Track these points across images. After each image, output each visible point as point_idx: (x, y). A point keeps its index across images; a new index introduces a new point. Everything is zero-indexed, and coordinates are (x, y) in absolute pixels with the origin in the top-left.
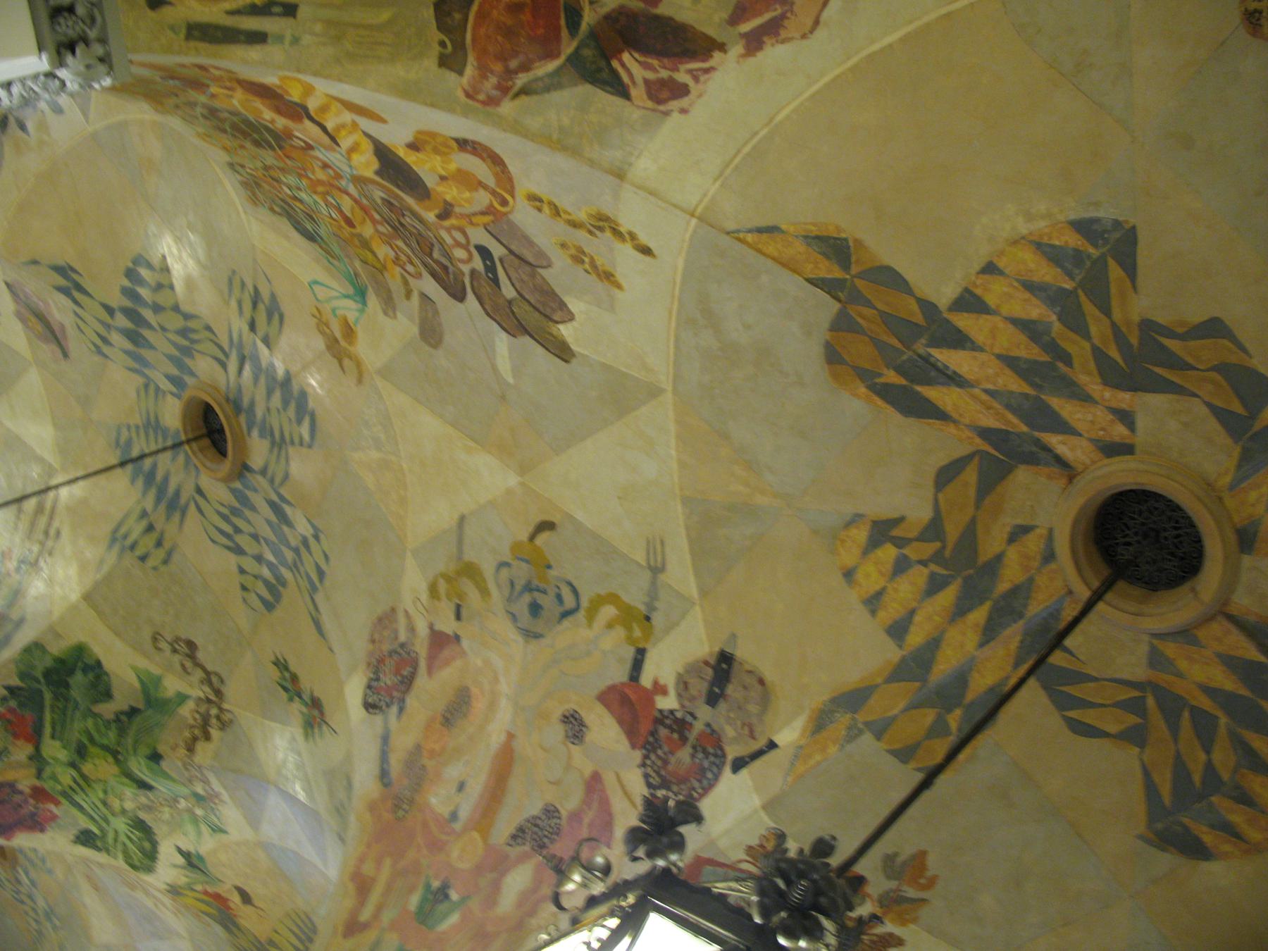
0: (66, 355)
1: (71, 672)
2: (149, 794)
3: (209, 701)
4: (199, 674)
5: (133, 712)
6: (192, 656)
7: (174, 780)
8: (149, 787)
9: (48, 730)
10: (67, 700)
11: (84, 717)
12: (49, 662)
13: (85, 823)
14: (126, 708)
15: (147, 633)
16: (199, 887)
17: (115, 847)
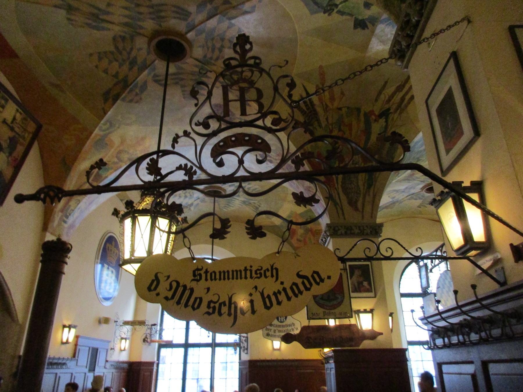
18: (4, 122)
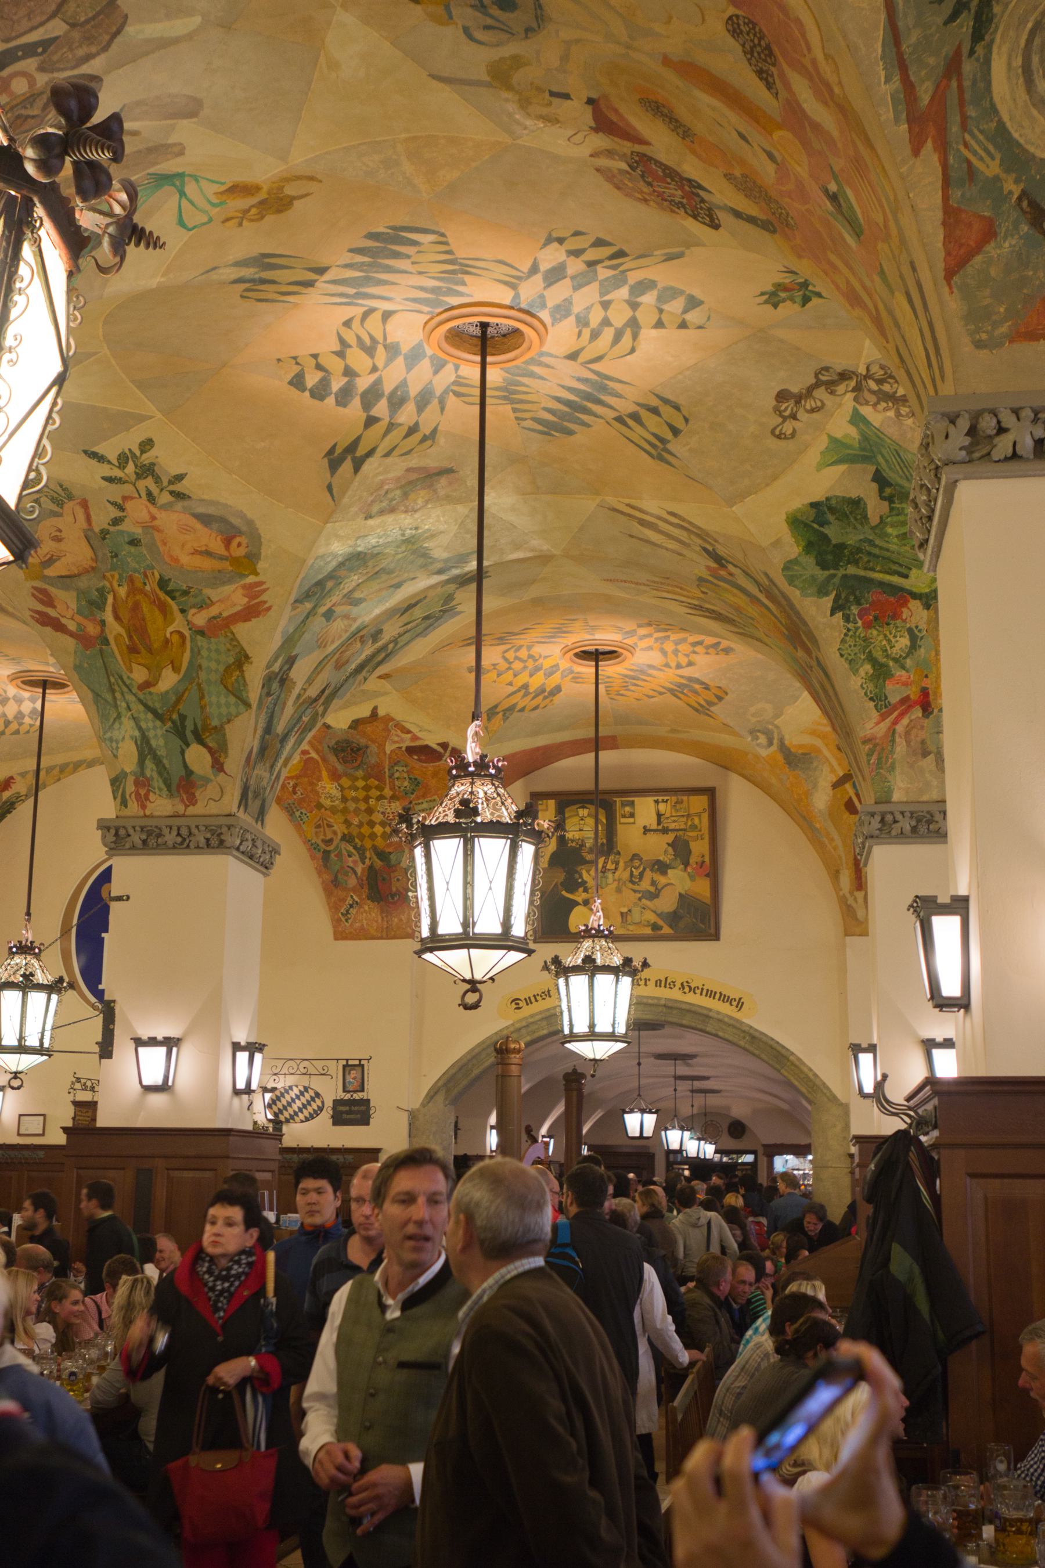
0: (449, 471)
1: (825, 538)
3: (858, 389)
4: (820, 393)
5: (879, 479)
6: (799, 399)
9: (895, 580)
10: (859, 550)
11: (884, 535)
12: (810, 561)
14: (875, 486)
15: (772, 443)
18: (646, 830)
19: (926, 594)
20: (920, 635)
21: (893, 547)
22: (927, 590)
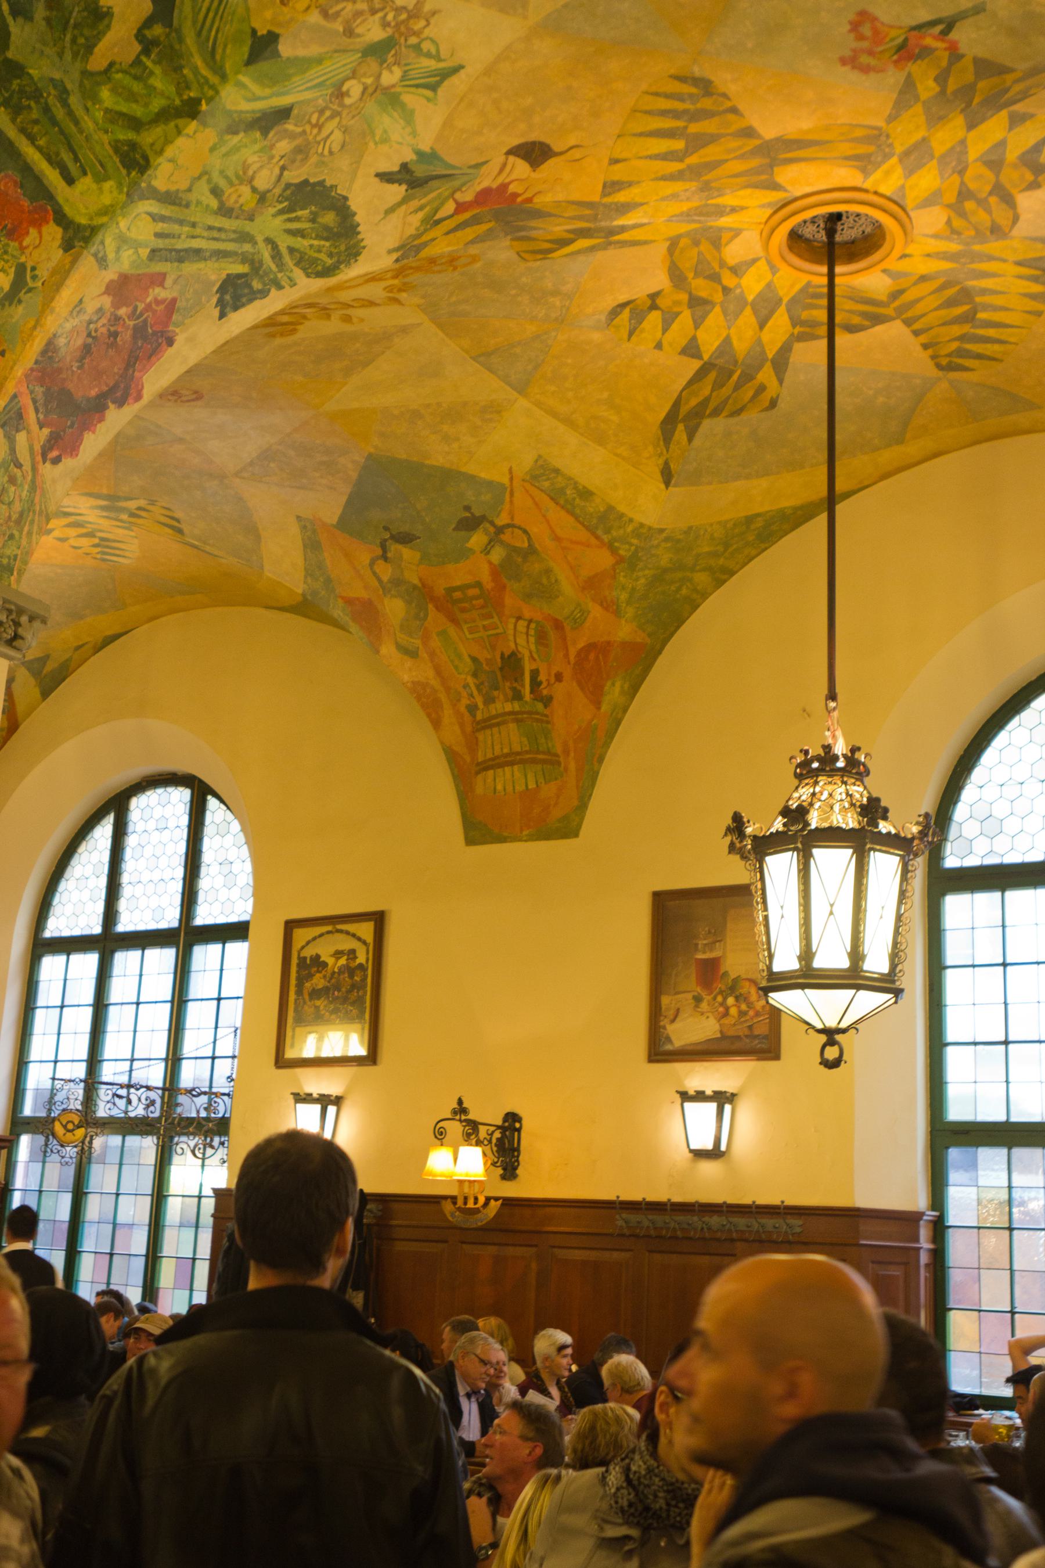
2: (290, 126)
7: (319, 60)
8: (284, 114)
9: (52, 176)
10: (37, 95)
11: (91, 96)
13: (215, 272)
16: (450, 207)
17: (281, 266)
19: (79, 225)
20: (31, 284)
21: (88, 124)
22: (83, 221)
